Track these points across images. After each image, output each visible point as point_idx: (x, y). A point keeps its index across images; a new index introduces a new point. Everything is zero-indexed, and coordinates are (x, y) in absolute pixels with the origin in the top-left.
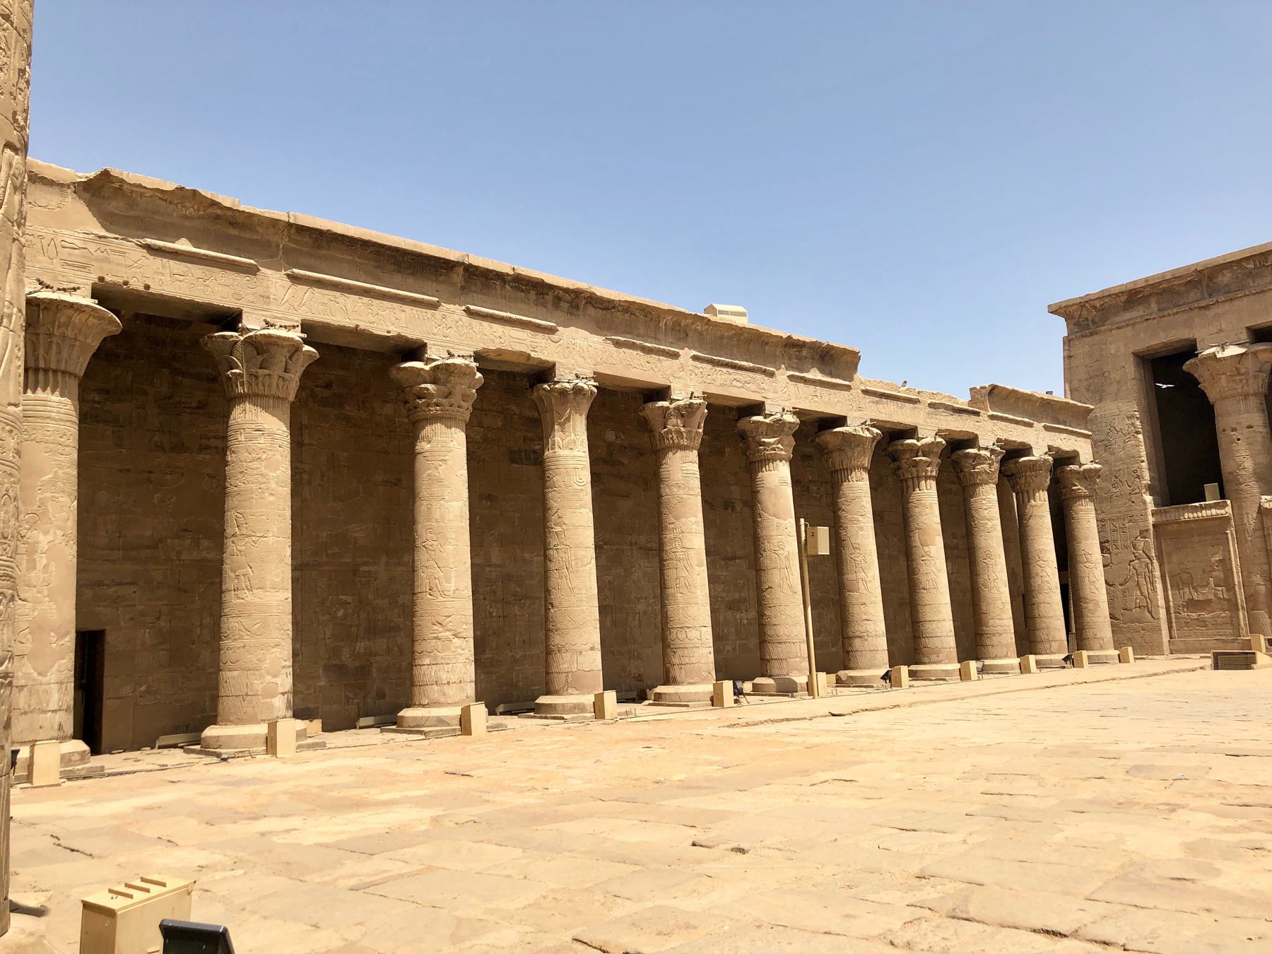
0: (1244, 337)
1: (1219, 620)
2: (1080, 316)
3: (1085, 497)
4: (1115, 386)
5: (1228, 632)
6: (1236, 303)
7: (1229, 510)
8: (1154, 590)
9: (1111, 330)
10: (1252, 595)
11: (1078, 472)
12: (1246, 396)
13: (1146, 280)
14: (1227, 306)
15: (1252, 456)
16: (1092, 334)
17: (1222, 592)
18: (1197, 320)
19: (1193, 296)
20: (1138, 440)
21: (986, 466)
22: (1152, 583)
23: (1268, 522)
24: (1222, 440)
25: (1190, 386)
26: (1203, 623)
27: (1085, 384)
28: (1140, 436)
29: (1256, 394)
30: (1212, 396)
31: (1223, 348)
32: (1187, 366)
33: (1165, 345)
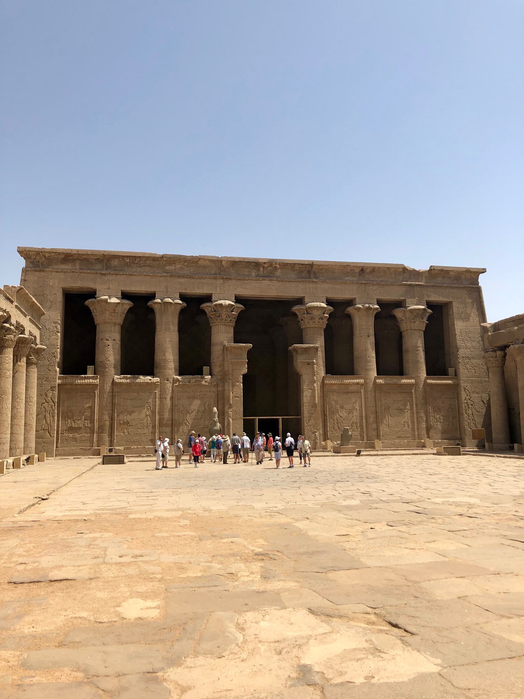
0: (120, 295)
1: (84, 438)
2: (35, 259)
3: (35, 364)
5: (87, 444)
6: (119, 277)
7: (98, 380)
8: (54, 421)
9: (52, 272)
10: (102, 426)
11: (34, 349)
12: (115, 324)
13: (78, 251)
14: (114, 277)
15: (114, 355)
16: (40, 271)
17: (88, 424)
19: (98, 266)
20: (58, 336)
21: (12, 336)
22: (53, 417)
23: (115, 389)
24: (99, 344)
25: (87, 314)
26: (75, 439)
28: (59, 334)
30: (98, 319)
31: (110, 298)
32: (88, 302)
33: (80, 288)
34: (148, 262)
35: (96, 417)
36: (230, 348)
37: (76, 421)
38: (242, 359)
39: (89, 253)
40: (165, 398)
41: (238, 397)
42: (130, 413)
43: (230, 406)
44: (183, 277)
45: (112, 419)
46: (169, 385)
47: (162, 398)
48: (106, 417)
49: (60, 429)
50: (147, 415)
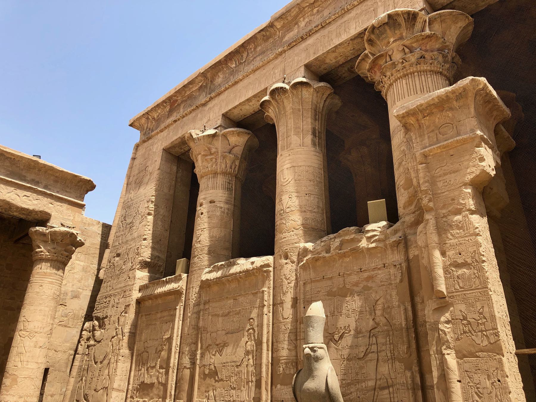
4: (148, 177)
6: (222, 97)
12: (215, 174)
15: (210, 228)
18: (199, 115)
27: (135, 178)
28: (150, 218)
29: (224, 173)
34: (259, 49)
35: (174, 361)
36: (412, 120)
37: (150, 370)
38: (458, 134)
39: (186, 83)
40: (282, 303)
41: (465, 265)
42: (221, 347)
43: (443, 303)
44: (310, 34)
45: (193, 363)
46: (289, 269)
47: (277, 304)
48: (186, 361)
49: (130, 387)
50: (247, 353)
